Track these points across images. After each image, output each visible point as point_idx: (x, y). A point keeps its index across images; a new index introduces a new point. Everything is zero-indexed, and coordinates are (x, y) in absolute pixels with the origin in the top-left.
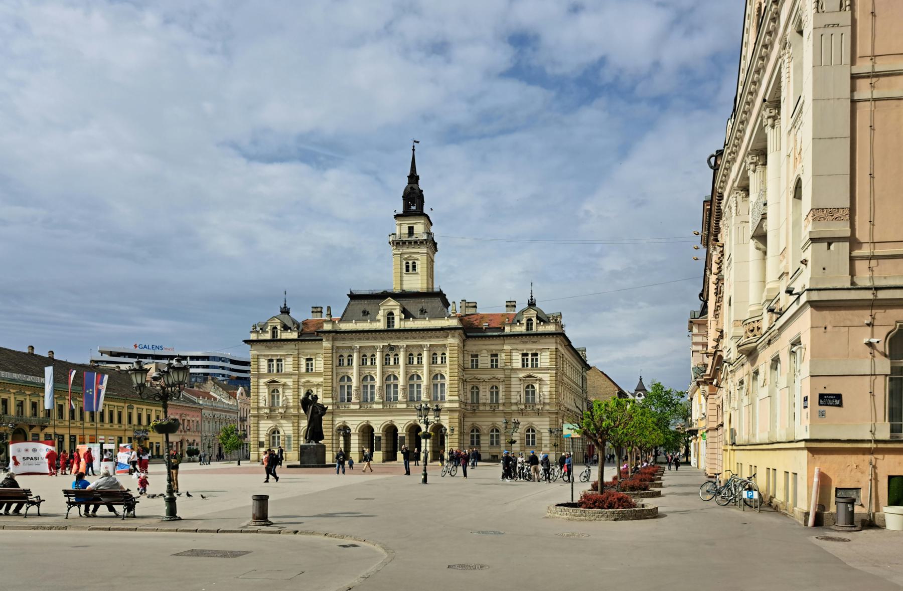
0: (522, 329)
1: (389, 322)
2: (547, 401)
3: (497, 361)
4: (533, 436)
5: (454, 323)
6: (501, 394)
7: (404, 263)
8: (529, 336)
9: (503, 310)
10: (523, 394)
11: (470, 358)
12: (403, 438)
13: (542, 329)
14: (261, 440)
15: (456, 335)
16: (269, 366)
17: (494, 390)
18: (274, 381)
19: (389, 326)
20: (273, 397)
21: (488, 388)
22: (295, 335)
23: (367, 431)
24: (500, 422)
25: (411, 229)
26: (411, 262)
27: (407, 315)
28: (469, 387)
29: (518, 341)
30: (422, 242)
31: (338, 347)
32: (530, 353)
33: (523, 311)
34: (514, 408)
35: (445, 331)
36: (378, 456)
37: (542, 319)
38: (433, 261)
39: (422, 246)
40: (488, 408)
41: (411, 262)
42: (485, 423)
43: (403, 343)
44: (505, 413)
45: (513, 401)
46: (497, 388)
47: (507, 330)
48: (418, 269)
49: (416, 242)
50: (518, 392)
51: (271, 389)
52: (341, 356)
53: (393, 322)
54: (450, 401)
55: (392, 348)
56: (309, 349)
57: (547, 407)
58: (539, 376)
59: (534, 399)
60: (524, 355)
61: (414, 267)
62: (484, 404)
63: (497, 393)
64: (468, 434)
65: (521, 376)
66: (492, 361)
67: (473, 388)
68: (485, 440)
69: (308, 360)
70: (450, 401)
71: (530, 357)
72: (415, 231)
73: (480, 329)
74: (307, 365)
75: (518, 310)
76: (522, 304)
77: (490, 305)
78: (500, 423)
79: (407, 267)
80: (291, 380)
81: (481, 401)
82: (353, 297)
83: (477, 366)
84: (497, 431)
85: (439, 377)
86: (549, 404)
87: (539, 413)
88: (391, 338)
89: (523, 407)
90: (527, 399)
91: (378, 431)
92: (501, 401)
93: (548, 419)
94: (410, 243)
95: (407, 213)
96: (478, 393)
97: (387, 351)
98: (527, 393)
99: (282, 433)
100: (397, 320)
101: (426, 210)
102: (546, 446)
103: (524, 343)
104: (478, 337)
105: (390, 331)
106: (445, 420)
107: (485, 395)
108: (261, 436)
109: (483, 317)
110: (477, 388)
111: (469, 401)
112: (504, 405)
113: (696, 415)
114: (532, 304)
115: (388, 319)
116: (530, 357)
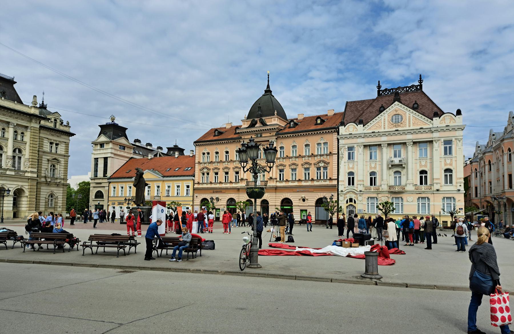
0: (51, 125)
2: (62, 177)
8: (54, 131)
13: (62, 128)
29: (49, 133)
32: (55, 142)
45: (43, 175)
50: (46, 169)
54: (32, 172)
57: (62, 182)
65: (48, 158)
70: (32, 172)
71: (54, 145)
85: (17, 151)
87: (58, 185)
90: (51, 174)
93: (62, 189)
98: (51, 169)
102: (60, 207)
103: (52, 135)
106: (26, 186)
116: (54, 145)
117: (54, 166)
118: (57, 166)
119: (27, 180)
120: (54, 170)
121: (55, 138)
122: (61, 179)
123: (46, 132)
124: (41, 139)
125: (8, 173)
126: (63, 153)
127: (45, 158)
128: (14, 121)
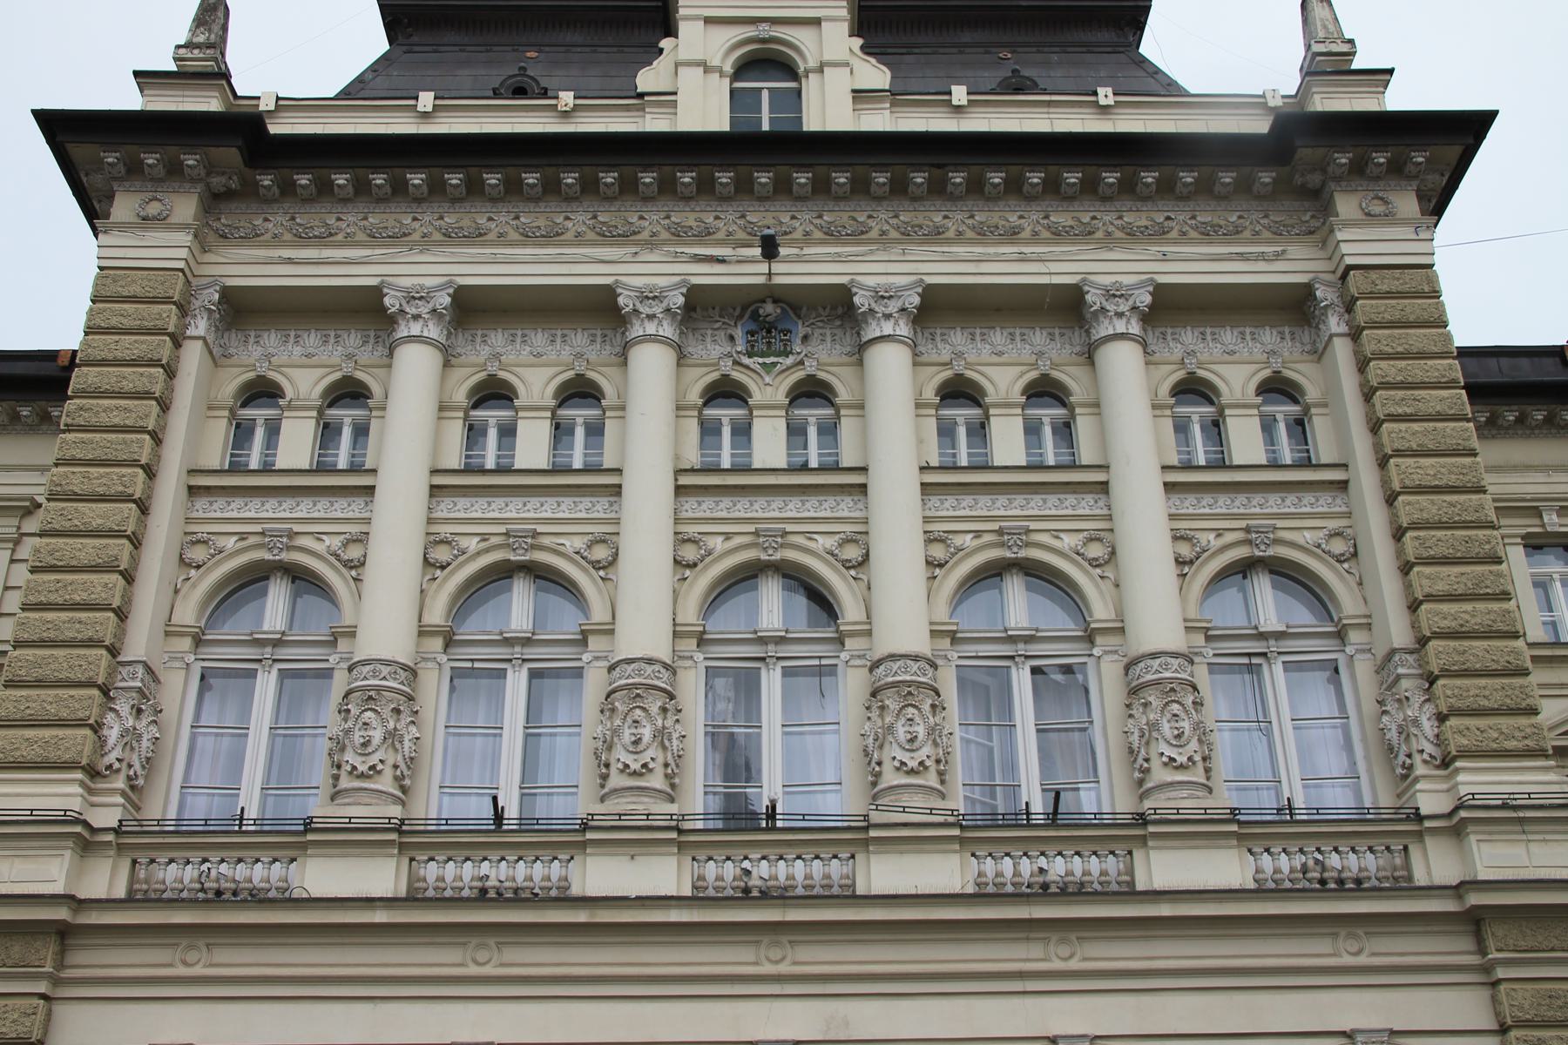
43: (883, 264)
52: (262, 391)
119: (1455, 949)
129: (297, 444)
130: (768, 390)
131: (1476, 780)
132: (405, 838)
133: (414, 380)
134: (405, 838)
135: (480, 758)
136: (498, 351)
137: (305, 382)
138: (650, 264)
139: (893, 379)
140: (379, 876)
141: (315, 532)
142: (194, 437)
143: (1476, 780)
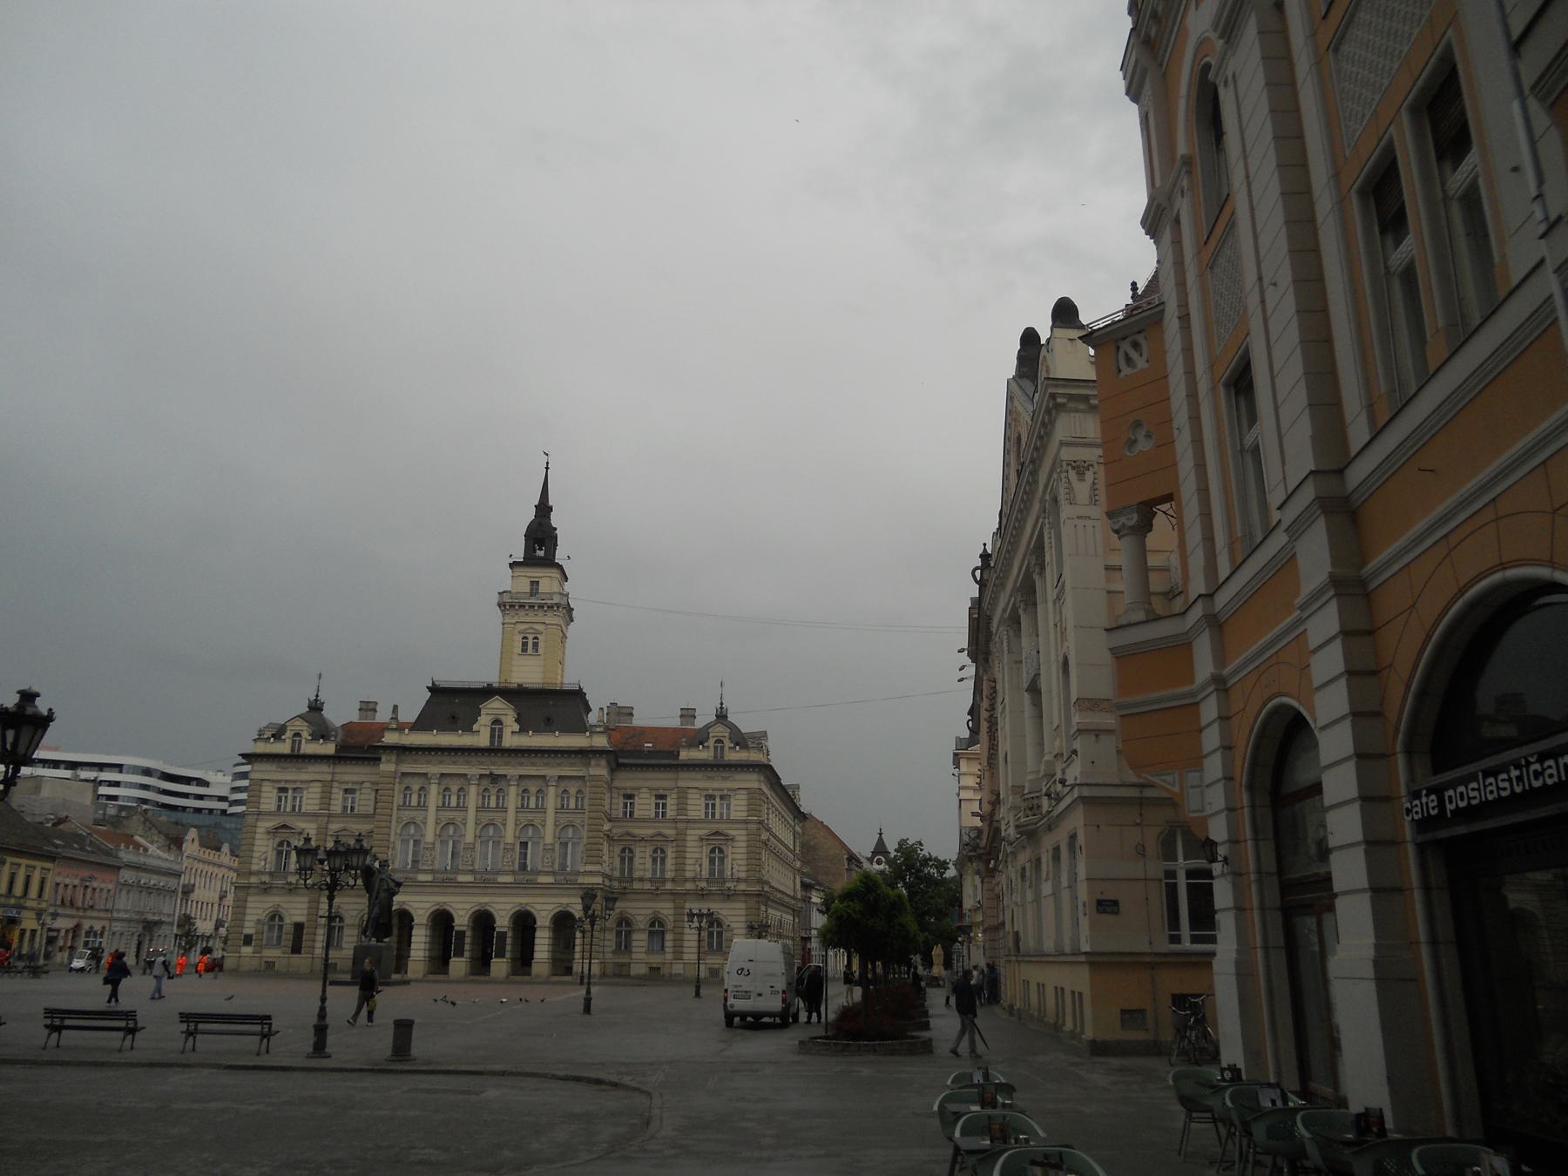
1: (492, 736)
2: (743, 875)
3: (664, 805)
4: (720, 934)
5: (601, 742)
6: (669, 862)
7: (519, 638)
8: (718, 766)
9: (675, 722)
10: (706, 862)
11: (621, 800)
12: (503, 936)
14: (247, 931)
15: (604, 762)
16: (280, 799)
17: (659, 856)
18: (284, 826)
19: (492, 742)
20: (279, 853)
21: (649, 850)
22: (329, 749)
23: (442, 921)
24: (666, 909)
25: (535, 584)
26: (531, 637)
27: (524, 726)
28: (617, 850)
29: (699, 776)
30: (551, 607)
31: (404, 774)
32: (717, 793)
33: (708, 726)
34: (689, 886)
35: (584, 754)
36: (458, 965)
37: (740, 740)
38: (565, 636)
39: (550, 614)
40: (647, 886)
41: (531, 637)
42: (640, 911)
43: (512, 770)
44: (673, 893)
45: (689, 875)
46: (663, 851)
47: (685, 755)
48: (541, 651)
49: (541, 607)
51: (278, 840)
53: (500, 737)
55: (494, 778)
56: (352, 774)
57: (742, 887)
58: (732, 832)
59: (721, 872)
60: (712, 797)
61: (536, 645)
62: (641, 880)
63: (663, 860)
64: (610, 930)
66: (657, 805)
67: (623, 851)
68: (640, 940)
69: (346, 791)
72: (541, 589)
73: (639, 753)
74: (345, 799)
75: (699, 723)
76: (704, 718)
77: (655, 712)
78: (666, 912)
79: (525, 645)
80: (314, 826)
81: (636, 874)
82: (435, 690)
83: (631, 814)
84: (661, 924)
86: (745, 881)
87: (729, 896)
88: (494, 764)
89: (704, 884)
90: (712, 872)
91: (462, 920)
92: (669, 875)
93: (743, 905)
94: (532, 607)
95: (530, 561)
96: (631, 859)
97: (485, 783)
98: (712, 861)
99: (287, 920)
100: (507, 733)
101: (560, 557)
103: (709, 778)
104: (637, 766)
105: (495, 751)
107: (643, 863)
108: (247, 924)
109: (643, 732)
110: (631, 851)
111: (617, 874)
112: (673, 880)
113: (968, 903)
114: (722, 716)
115: (493, 730)
117: (721, 851)
118: (729, 850)
120: (722, 860)
121: (716, 784)
122: (739, 880)
123: (692, 775)
124: (683, 794)
125: (542, 879)
126: (742, 815)
127: (693, 834)
128: (552, 772)
129: (415, 798)
130: (494, 791)
131: (589, 868)
132: (433, 871)
133: (434, 789)
134: (433, 871)
135: (442, 860)
136: (446, 782)
137: (416, 787)
138: (474, 770)
139: (513, 791)
140: (429, 878)
141: (419, 816)
142: (398, 799)
143: (589, 868)
